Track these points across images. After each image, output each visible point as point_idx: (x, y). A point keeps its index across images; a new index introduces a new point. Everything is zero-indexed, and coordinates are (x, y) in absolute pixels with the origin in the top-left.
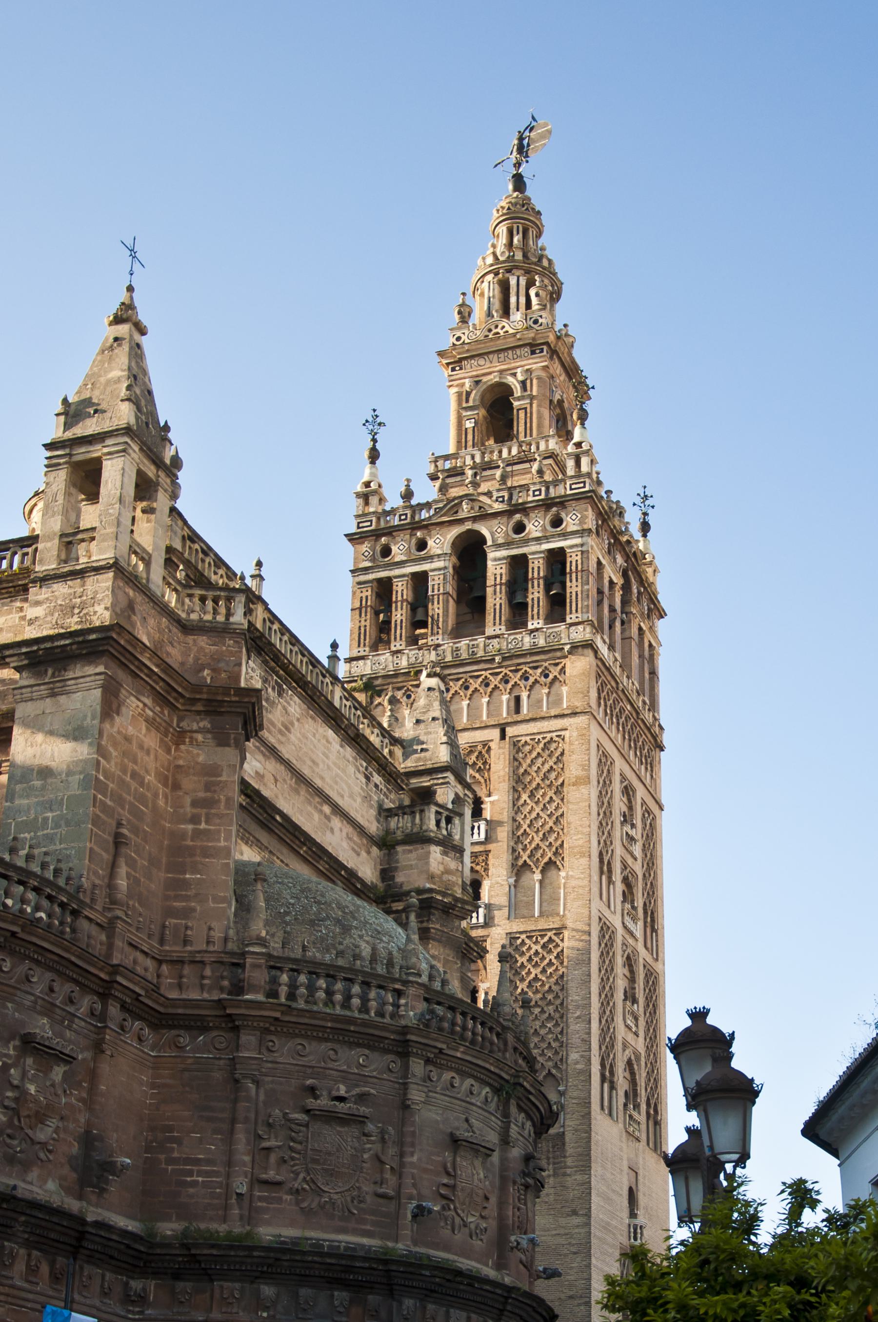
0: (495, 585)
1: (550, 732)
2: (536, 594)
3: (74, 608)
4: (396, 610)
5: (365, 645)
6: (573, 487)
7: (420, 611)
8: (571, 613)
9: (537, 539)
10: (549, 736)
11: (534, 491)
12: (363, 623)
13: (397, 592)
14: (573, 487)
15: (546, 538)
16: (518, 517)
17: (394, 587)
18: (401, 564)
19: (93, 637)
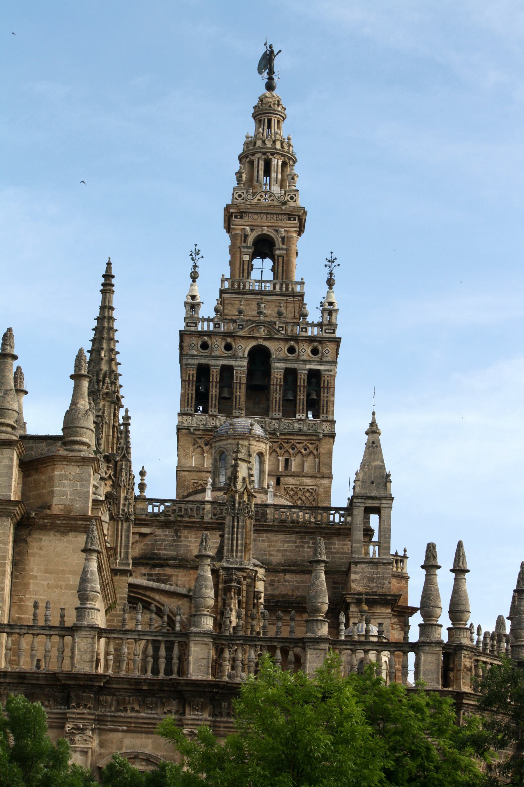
0: (277, 385)
1: (307, 485)
2: (302, 397)
3: (374, 579)
4: (212, 388)
5: (191, 406)
6: (327, 331)
7: (226, 390)
8: (323, 413)
9: (304, 361)
10: (306, 487)
11: (302, 328)
12: (190, 392)
13: (213, 375)
14: (327, 331)
15: (310, 362)
16: (292, 343)
17: (211, 372)
18: (216, 357)
19: (389, 598)
